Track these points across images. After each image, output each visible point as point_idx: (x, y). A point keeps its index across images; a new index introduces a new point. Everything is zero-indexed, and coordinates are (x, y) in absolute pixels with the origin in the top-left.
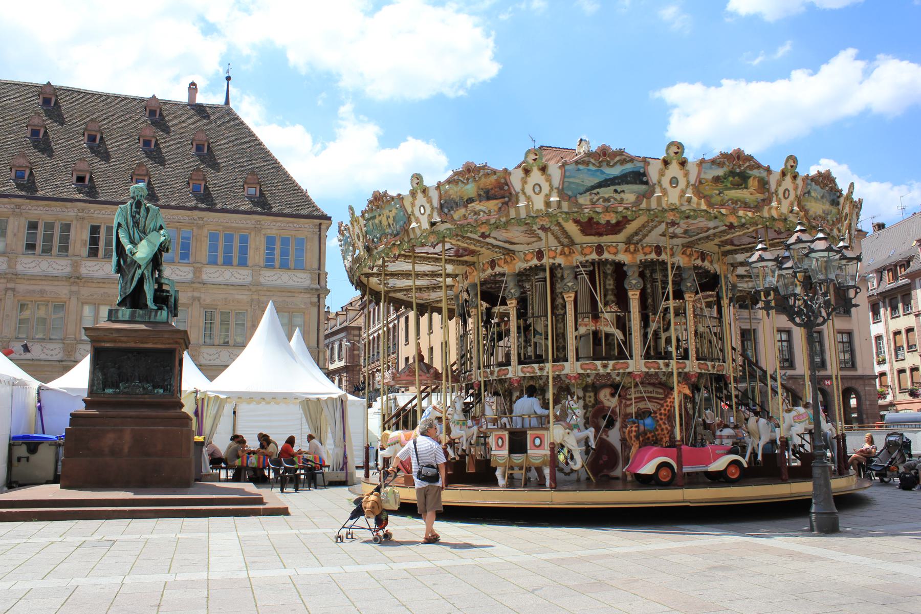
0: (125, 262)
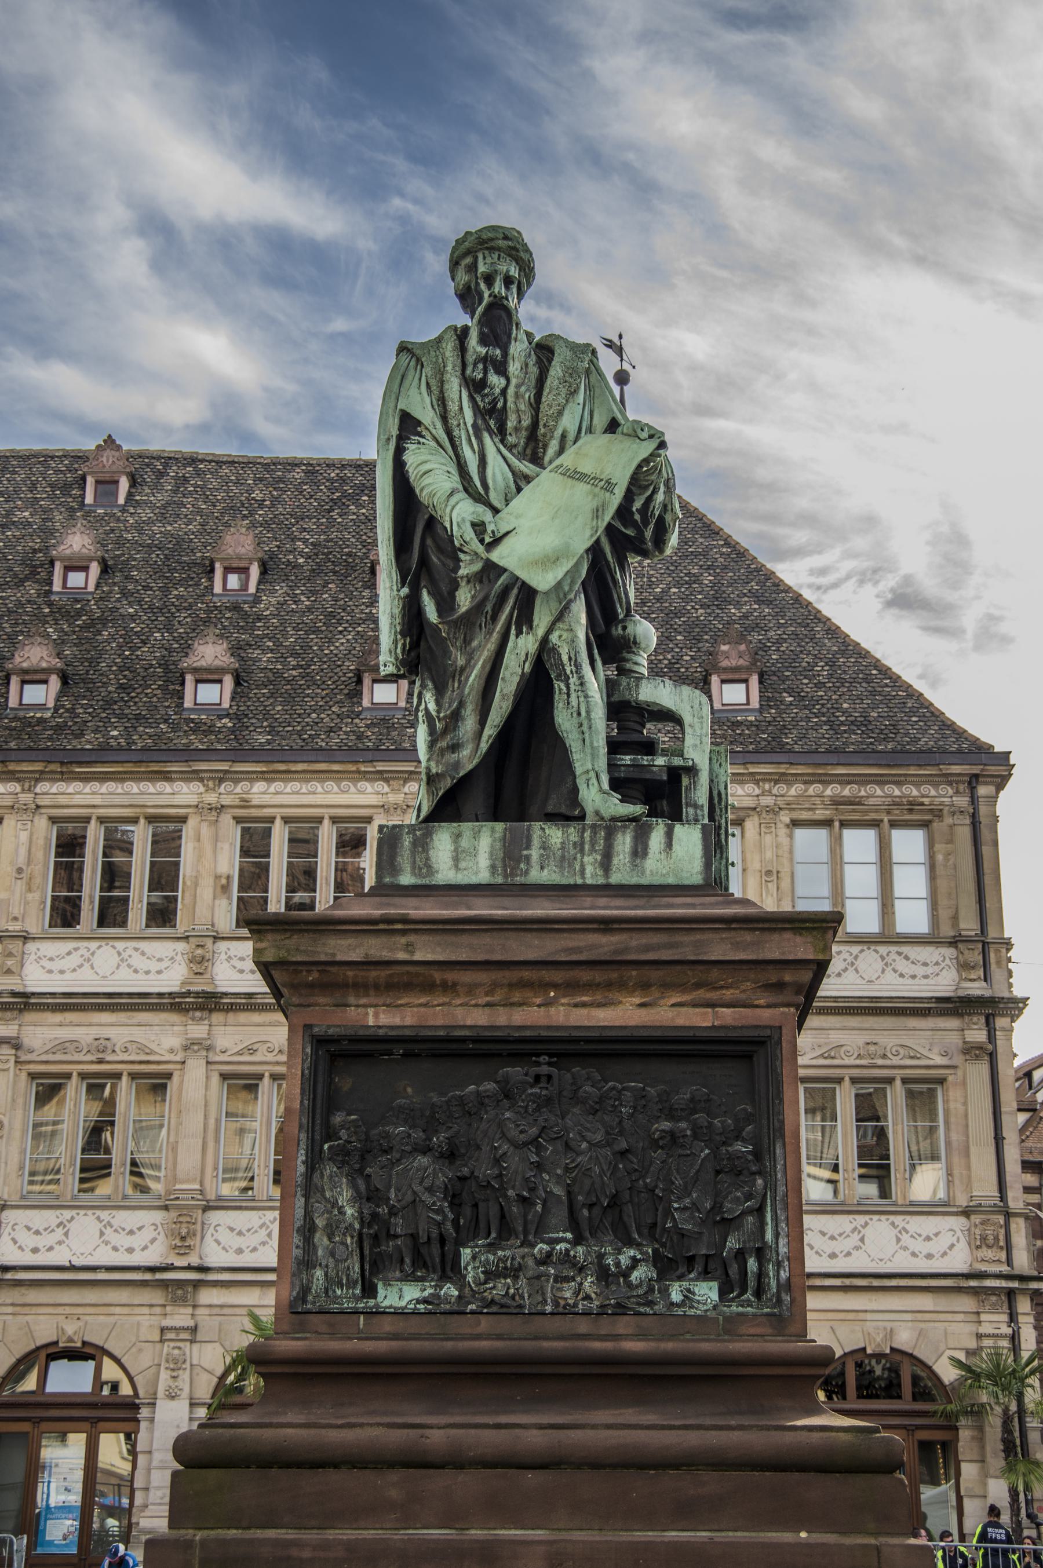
0: (446, 604)
